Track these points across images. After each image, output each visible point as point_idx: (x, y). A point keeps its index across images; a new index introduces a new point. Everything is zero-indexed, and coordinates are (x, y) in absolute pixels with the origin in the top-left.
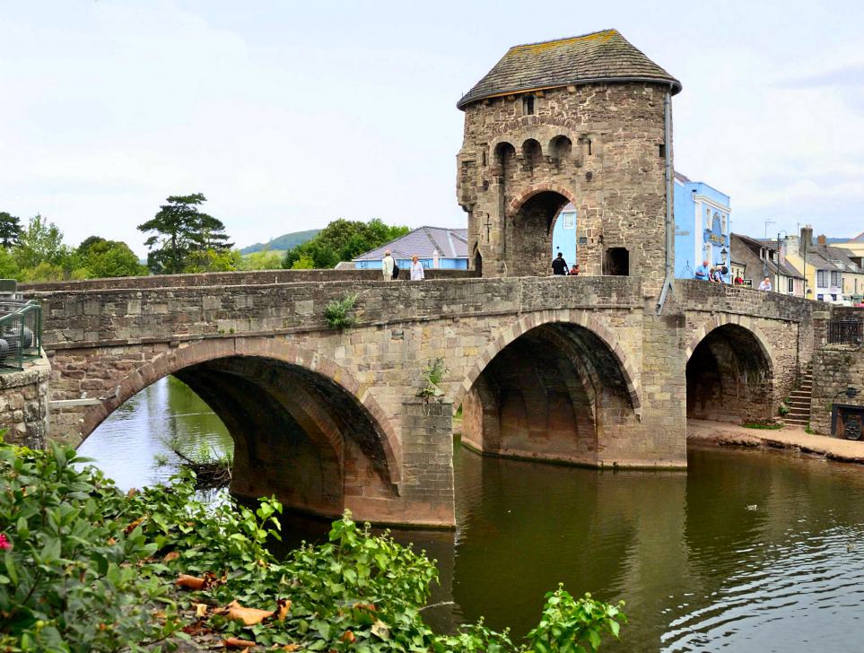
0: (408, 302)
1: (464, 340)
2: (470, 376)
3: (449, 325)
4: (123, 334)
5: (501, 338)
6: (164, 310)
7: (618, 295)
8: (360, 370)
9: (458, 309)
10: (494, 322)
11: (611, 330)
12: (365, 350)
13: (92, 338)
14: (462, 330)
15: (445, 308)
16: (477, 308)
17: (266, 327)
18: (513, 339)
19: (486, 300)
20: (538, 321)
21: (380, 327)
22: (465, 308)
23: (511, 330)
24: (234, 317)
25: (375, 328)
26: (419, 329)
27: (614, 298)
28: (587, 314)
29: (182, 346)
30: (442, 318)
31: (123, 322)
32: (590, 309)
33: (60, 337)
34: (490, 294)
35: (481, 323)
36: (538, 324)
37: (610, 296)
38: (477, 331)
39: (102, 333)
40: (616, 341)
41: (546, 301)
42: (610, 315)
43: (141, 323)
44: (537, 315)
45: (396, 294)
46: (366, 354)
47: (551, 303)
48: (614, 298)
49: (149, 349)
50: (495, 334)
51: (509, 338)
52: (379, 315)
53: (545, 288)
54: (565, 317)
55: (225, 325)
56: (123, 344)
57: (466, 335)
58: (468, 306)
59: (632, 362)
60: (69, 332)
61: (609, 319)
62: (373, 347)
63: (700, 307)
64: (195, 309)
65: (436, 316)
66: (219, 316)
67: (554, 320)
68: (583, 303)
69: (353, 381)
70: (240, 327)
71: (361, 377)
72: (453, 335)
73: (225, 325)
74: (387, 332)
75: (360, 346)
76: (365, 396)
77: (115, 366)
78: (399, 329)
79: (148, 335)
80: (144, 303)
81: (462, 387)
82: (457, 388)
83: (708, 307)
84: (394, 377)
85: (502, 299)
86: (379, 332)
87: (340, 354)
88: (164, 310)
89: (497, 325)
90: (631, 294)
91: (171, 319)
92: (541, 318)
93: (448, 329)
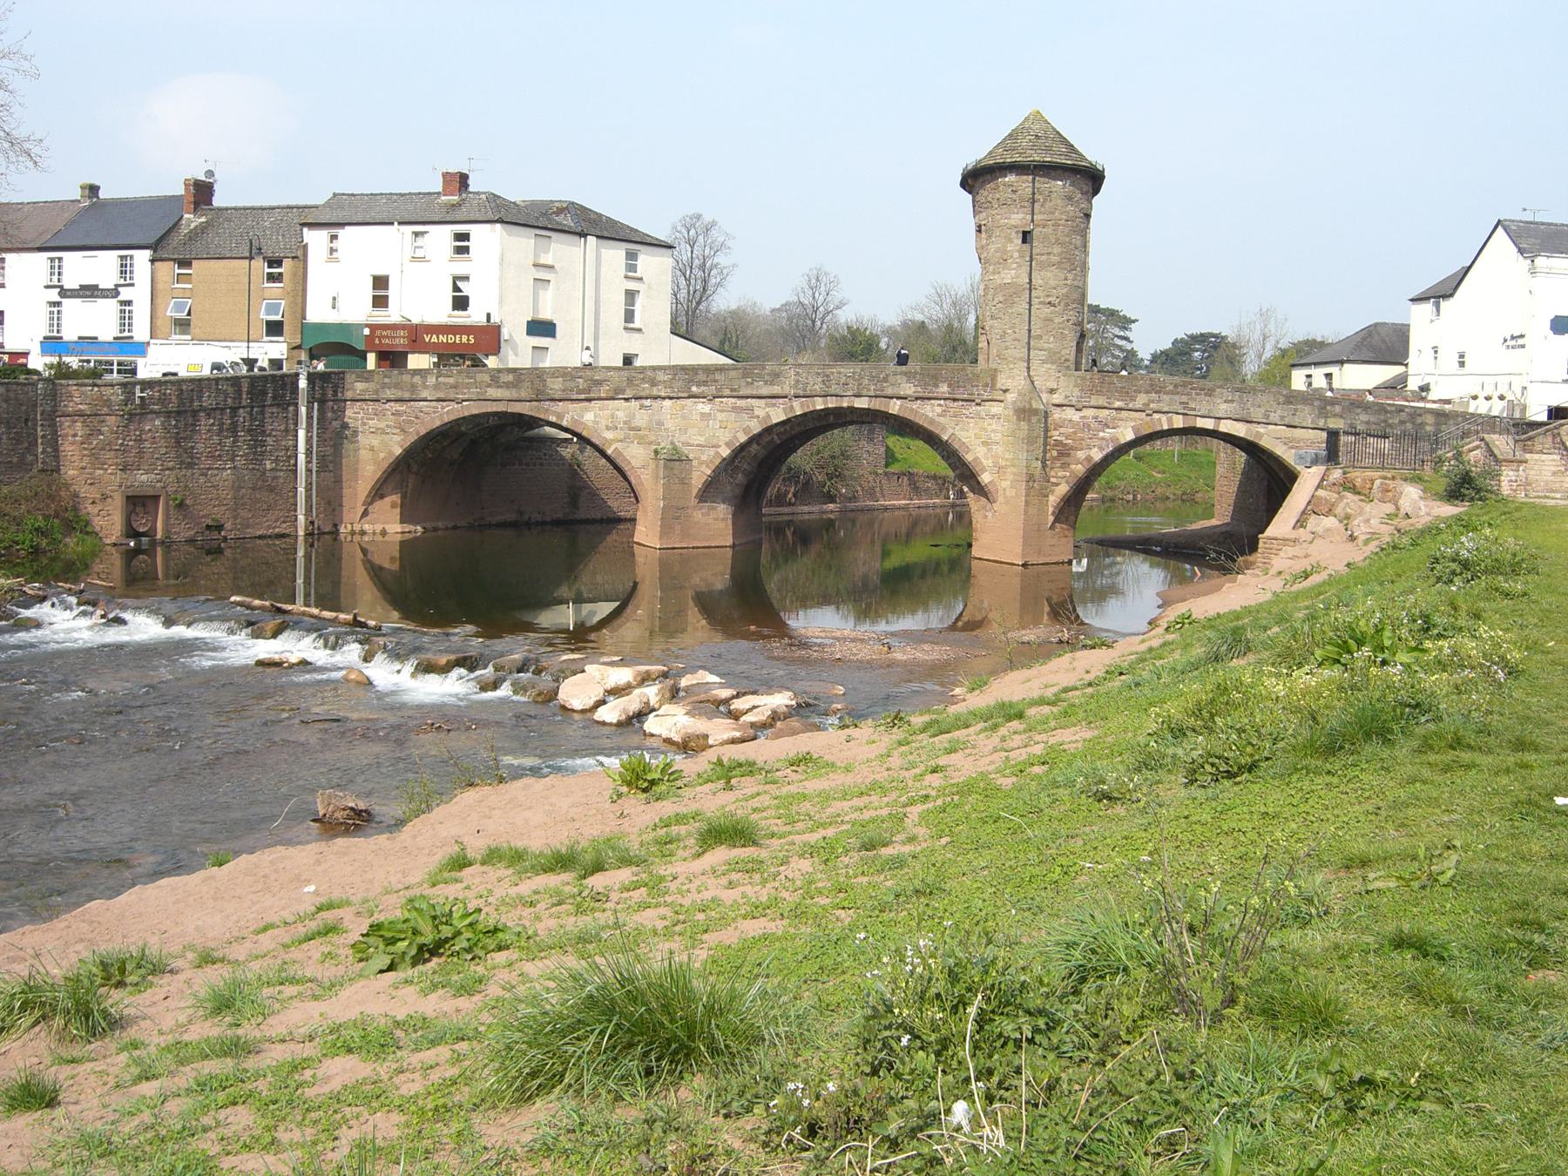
1: (720, 416)
2: (727, 444)
4: (424, 394)
6: (451, 380)
9: (712, 390)
11: (942, 420)
13: (407, 395)
20: (819, 405)
21: (626, 400)
23: (780, 410)
26: (667, 403)
27: (944, 389)
31: (426, 387)
38: (735, 409)
39: (413, 392)
43: (437, 387)
47: (834, 389)
48: (944, 389)
52: (623, 392)
53: (828, 376)
55: (493, 392)
57: (722, 411)
60: (393, 391)
61: (939, 410)
63: (1118, 404)
66: (489, 386)
67: (845, 405)
68: (889, 391)
71: (609, 435)
73: (493, 392)
78: (648, 402)
79: (441, 395)
83: (1138, 404)
84: (641, 437)
88: (451, 380)
91: (455, 387)
93: (700, 406)
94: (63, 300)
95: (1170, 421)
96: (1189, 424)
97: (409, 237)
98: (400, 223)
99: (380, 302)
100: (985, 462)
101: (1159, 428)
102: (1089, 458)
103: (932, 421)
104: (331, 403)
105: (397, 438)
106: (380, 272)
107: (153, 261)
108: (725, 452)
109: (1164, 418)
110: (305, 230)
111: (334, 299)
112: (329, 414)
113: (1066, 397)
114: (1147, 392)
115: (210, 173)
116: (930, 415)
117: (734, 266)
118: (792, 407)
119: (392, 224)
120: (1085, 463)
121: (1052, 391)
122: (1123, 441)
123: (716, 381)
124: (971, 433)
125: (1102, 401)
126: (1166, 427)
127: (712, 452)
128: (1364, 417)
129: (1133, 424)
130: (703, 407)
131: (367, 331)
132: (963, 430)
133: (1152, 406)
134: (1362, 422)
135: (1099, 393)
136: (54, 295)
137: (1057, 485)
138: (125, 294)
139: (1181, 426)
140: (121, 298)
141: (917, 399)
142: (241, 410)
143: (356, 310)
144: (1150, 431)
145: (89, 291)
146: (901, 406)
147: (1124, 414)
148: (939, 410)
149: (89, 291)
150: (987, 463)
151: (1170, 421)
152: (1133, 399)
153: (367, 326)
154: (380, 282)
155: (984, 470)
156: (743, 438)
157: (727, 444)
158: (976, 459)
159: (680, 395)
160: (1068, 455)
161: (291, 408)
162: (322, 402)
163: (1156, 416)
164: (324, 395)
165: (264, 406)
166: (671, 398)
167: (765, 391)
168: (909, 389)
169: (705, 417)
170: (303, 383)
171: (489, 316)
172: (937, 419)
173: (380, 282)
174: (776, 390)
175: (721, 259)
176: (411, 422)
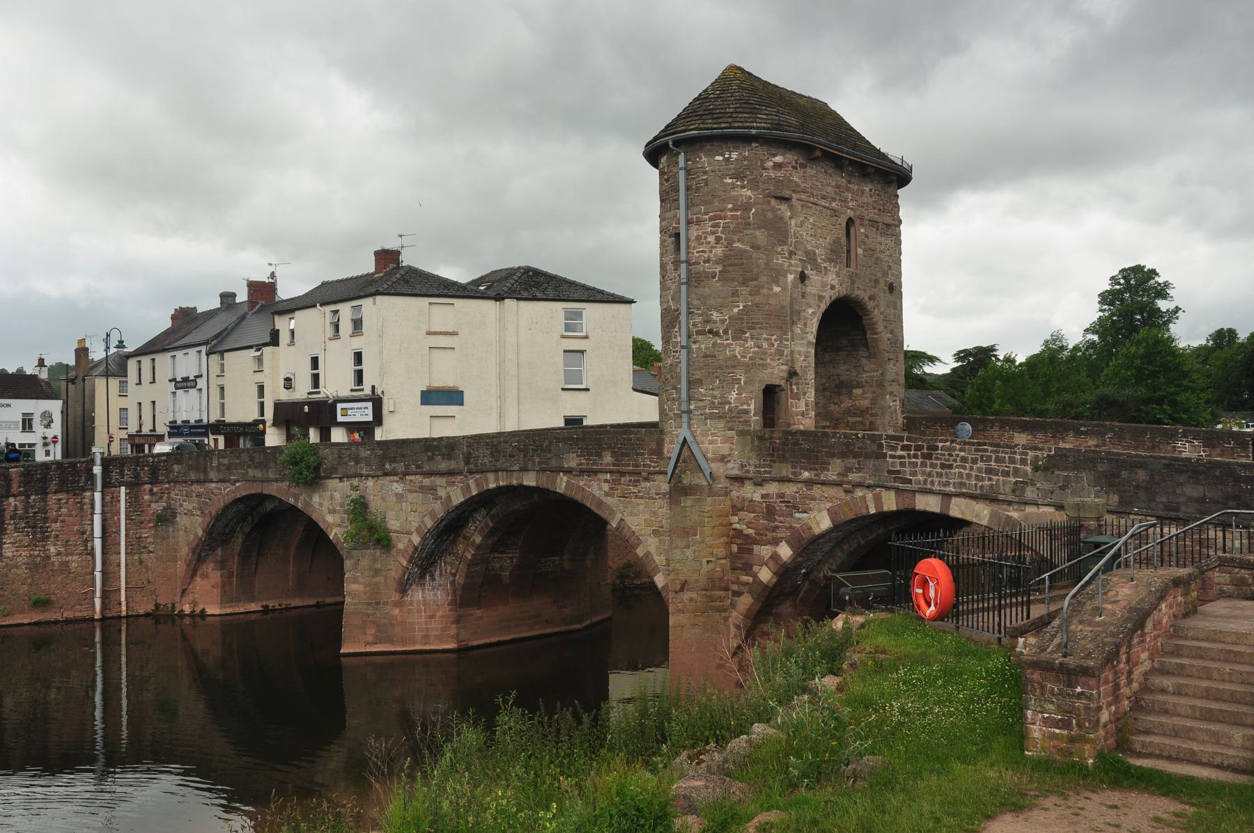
0: (357, 461)
1: (411, 497)
2: (418, 530)
3: (397, 482)
5: (449, 497)
7: (614, 454)
8: (329, 513)
9: (400, 467)
10: (440, 481)
11: (609, 500)
12: (332, 498)
13: (202, 477)
14: (408, 487)
15: (387, 466)
16: (418, 467)
17: (271, 476)
18: (462, 499)
19: (425, 458)
21: (341, 479)
22: (407, 467)
23: (459, 491)
24: (256, 468)
25: (338, 480)
26: (370, 483)
27: (608, 458)
28: (565, 478)
29: (237, 484)
30: (386, 474)
32: (568, 471)
33: (192, 475)
34: (430, 454)
35: (427, 482)
36: (492, 486)
37: (599, 455)
38: (423, 489)
40: (619, 516)
41: (497, 461)
42: (606, 481)
44: (491, 476)
45: (348, 453)
46: (332, 500)
48: (608, 458)
49: (226, 485)
50: (442, 493)
51: (458, 498)
53: (496, 446)
54: (530, 480)
56: (212, 481)
57: (411, 491)
58: (409, 465)
59: (652, 549)
61: (606, 487)
62: (337, 495)
63: (806, 474)
64: (238, 461)
65: (379, 473)
66: (249, 467)
67: (515, 482)
68: (554, 463)
69: (325, 521)
70: (258, 474)
71: (330, 518)
72: (400, 490)
73: (251, 472)
74: (346, 484)
75: (329, 493)
76: (333, 534)
77: (212, 493)
80: (219, 458)
81: (410, 541)
82: (406, 541)
83: (832, 475)
85: (443, 458)
86: (341, 484)
87: (316, 499)
89: (444, 484)
90: (642, 454)
91: (229, 468)
92: (496, 480)
93: (395, 485)
94: (178, 391)
95: (878, 500)
96: (905, 505)
97: (329, 316)
98: (321, 305)
99: (316, 379)
100: (657, 558)
101: (864, 512)
102: (775, 557)
103: (600, 504)
104: (147, 487)
105: (200, 519)
106: (314, 353)
107: (208, 355)
108: (416, 540)
109: (870, 496)
110: (276, 317)
111: (288, 380)
112: (147, 497)
113: (742, 466)
114: (843, 456)
115: (273, 275)
116: (597, 493)
117: (1177, 309)
118: (468, 486)
119: (315, 306)
120: (771, 563)
121: (723, 459)
122: (817, 531)
123: (404, 456)
124: (643, 517)
125: (786, 471)
126: (872, 511)
127: (405, 539)
128: (1192, 491)
129: (829, 505)
130: (398, 488)
131: (306, 409)
132: (631, 514)
133: (851, 477)
134: (1190, 499)
135: (783, 459)
136: (172, 386)
137: (738, 594)
138: (202, 383)
139: (894, 508)
140: (198, 387)
141: (582, 472)
142: (11, 500)
143: (302, 391)
144: (852, 516)
145: (185, 384)
146: (568, 483)
147: (817, 491)
148: (606, 487)
149: (185, 384)
150: (659, 560)
151: (878, 500)
152: (824, 467)
153: (308, 403)
154: (315, 362)
155: (656, 570)
156: (429, 523)
157: (418, 530)
158: (648, 554)
159: (379, 473)
160: (750, 551)
161: (88, 494)
162: (133, 486)
163: (859, 493)
164: (137, 476)
165: (47, 494)
166: (373, 477)
167: (443, 465)
168: (572, 461)
169: (400, 497)
170: (97, 470)
171: (373, 387)
172: (604, 499)
173: (315, 362)
174: (453, 465)
175: (1163, 305)
176: (206, 503)
